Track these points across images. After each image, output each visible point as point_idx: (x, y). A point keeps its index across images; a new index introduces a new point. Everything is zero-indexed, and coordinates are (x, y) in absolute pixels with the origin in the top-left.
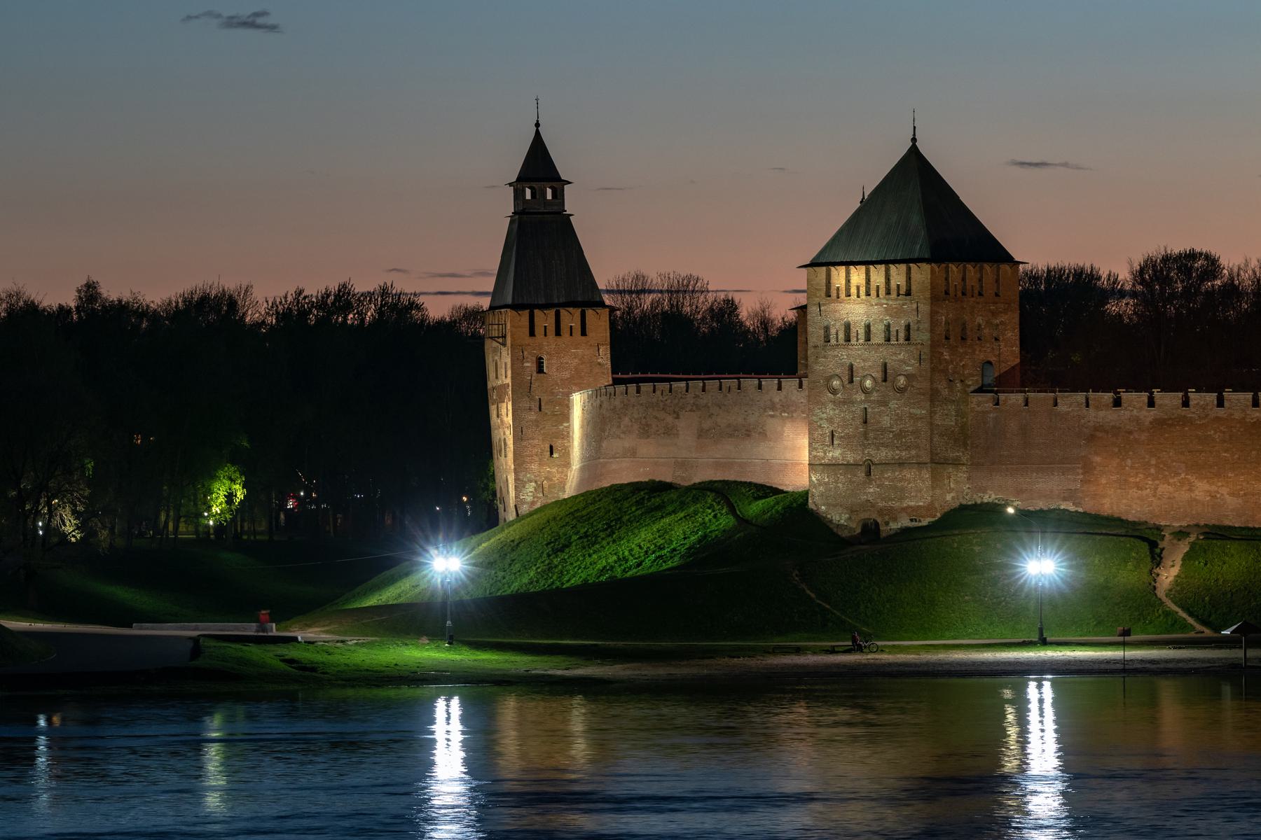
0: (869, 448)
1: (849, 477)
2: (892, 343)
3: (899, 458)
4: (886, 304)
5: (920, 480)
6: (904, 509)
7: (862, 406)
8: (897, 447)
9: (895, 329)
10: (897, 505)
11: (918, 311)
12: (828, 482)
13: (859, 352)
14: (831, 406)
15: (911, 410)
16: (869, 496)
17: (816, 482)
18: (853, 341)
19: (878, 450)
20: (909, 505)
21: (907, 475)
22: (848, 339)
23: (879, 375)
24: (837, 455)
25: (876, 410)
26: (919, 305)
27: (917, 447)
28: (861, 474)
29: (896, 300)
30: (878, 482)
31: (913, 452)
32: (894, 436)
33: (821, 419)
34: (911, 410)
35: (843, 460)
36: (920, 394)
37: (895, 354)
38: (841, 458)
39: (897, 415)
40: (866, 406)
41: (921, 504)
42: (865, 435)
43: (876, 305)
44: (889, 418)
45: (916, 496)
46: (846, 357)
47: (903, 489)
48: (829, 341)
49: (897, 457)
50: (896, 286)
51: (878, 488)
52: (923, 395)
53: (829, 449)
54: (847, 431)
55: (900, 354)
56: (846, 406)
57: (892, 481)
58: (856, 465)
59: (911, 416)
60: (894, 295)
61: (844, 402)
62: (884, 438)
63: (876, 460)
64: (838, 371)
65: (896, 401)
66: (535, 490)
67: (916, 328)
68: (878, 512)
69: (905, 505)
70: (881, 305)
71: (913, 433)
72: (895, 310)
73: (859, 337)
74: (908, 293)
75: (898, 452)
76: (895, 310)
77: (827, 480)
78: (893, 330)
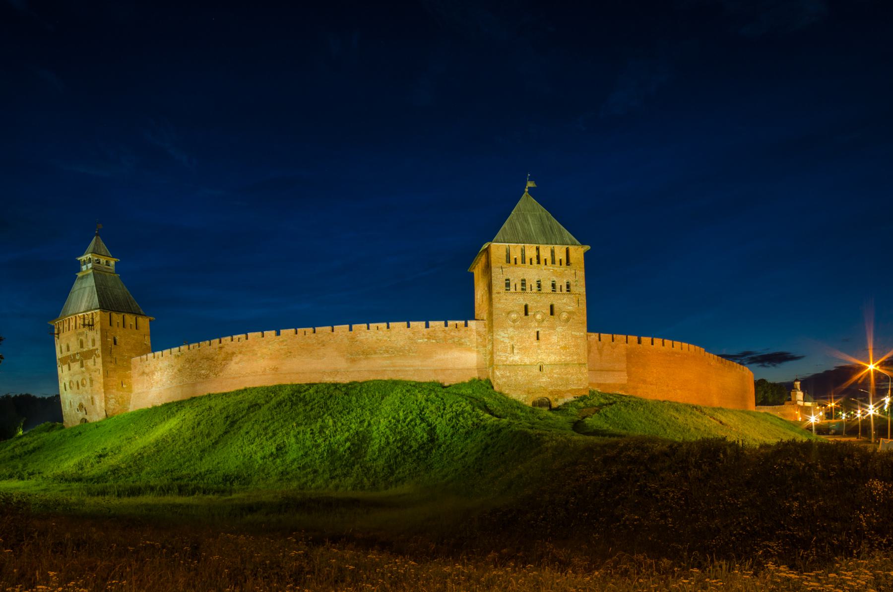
2: (557, 292)
3: (565, 361)
4: (553, 269)
6: (568, 391)
7: (537, 330)
9: (559, 285)
11: (575, 275)
12: (510, 377)
13: (533, 297)
14: (511, 329)
15: (573, 333)
16: (542, 383)
18: (528, 290)
25: (547, 332)
27: (578, 354)
29: (560, 267)
31: (575, 357)
33: (503, 337)
34: (573, 333)
35: (521, 362)
36: (580, 323)
37: (560, 299)
38: (520, 361)
39: (563, 335)
40: (538, 330)
41: (582, 388)
43: (545, 269)
45: (578, 383)
47: (567, 379)
49: (563, 360)
51: (549, 378)
52: (581, 324)
53: (510, 356)
54: (524, 345)
55: (563, 299)
57: (560, 374)
58: (531, 365)
61: (522, 327)
64: (516, 308)
65: (561, 327)
67: (574, 285)
68: (549, 393)
69: (569, 388)
70: (549, 270)
71: (574, 346)
73: (532, 288)
74: (568, 263)
75: (563, 357)
76: (559, 273)
77: (508, 374)
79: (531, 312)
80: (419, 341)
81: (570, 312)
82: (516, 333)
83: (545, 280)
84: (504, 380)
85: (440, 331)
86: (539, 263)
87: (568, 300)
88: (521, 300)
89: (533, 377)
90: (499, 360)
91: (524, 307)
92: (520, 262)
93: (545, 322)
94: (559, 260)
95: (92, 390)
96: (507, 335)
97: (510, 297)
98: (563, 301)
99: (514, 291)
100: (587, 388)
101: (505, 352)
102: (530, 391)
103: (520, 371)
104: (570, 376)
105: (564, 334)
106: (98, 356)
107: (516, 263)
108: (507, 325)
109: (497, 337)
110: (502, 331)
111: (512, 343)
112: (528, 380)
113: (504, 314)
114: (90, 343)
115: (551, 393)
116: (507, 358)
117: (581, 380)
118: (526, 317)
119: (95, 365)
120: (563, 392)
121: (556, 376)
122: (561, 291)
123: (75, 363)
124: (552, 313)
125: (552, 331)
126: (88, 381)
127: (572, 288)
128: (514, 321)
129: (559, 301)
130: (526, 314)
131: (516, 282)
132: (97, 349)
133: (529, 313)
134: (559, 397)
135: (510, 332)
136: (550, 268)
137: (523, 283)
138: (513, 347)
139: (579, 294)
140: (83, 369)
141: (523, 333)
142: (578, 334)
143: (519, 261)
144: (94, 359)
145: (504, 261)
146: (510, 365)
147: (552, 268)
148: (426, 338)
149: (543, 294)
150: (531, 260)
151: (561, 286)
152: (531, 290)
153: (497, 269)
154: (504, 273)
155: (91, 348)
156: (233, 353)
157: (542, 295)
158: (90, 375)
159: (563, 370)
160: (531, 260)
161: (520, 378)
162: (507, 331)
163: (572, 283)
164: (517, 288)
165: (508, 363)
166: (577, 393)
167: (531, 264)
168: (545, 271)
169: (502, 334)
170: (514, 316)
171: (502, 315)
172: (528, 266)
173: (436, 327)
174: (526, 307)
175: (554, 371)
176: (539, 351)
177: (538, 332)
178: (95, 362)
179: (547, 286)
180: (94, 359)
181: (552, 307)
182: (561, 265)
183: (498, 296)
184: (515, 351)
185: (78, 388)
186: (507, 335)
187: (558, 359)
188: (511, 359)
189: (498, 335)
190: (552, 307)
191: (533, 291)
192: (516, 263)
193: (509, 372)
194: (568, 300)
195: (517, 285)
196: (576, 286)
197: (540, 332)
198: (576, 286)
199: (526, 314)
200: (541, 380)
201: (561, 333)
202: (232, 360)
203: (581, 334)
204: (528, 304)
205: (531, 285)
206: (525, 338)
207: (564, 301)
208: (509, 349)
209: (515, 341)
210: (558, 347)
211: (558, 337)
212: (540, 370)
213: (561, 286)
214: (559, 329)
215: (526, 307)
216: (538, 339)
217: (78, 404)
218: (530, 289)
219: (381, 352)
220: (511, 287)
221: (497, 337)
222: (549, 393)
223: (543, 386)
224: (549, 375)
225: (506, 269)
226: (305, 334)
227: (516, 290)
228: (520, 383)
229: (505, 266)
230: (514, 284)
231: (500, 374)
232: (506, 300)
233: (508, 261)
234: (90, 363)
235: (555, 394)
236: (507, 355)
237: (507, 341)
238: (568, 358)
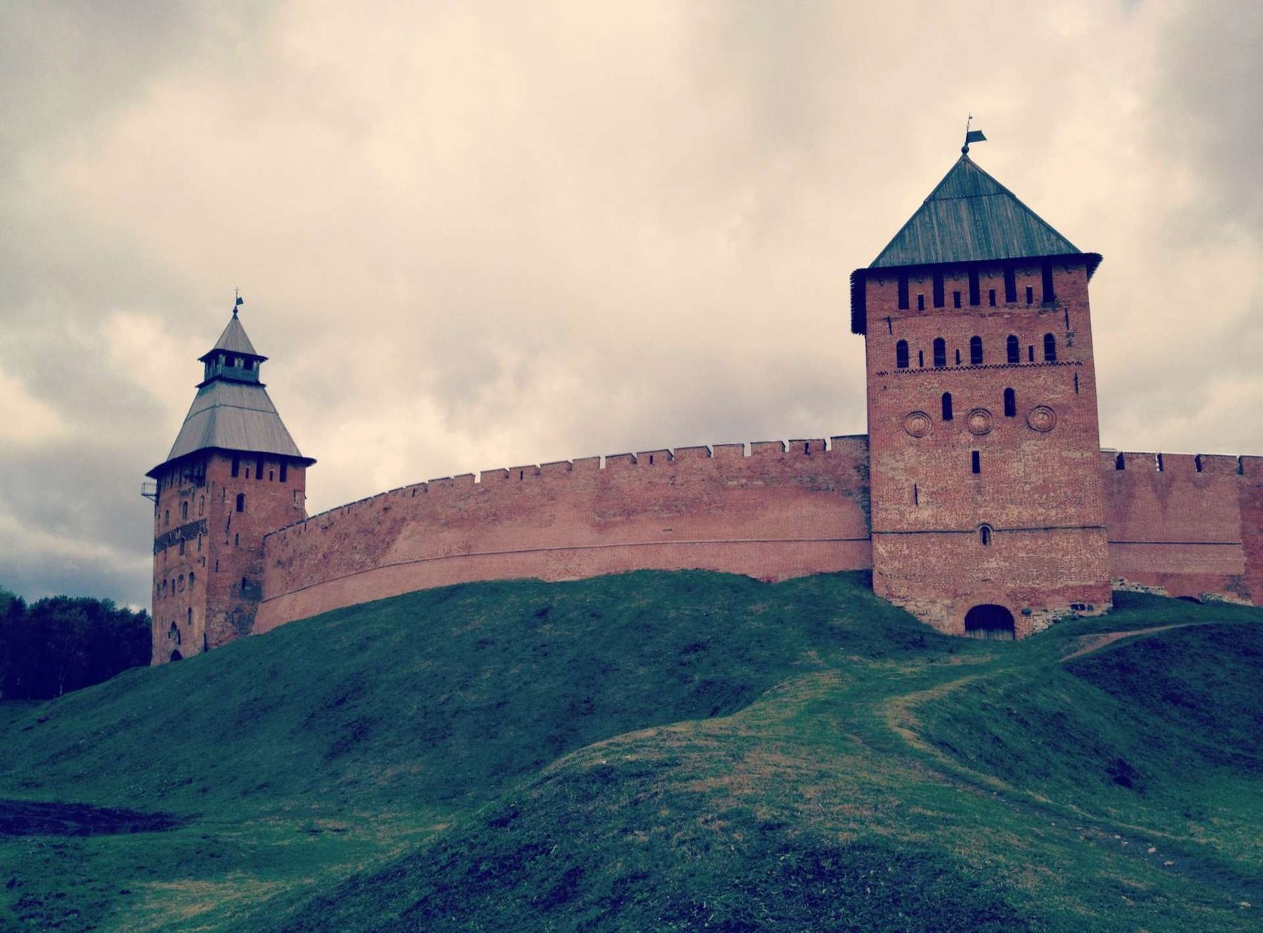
0: (986, 506)
1: (949, 546)
2: (1021, 364)
4: (1009, 314)
5: (1087, 549)
7: (971, 450)
8: (1039, 504)
10: (1045, 586)
13: (962, 379)
17: (885, 555)
18: (951, 362)
19: (1004, 508)
20: (1066, 585)
21: (1060, 543)
22: (940, 361)
23: (1000, 408)
24: (926, 517)
26: (1069, 312)
27: (1080, 503)
28: (974, 542)
29: (1027, 307)
30: (1005, 553)
31: (1072, 511)
32: (1032, 489)
34: (1064, 454)
37: (1028, 378)
38: (933, 521)
39: (1039, 459)
40: (976, 449)
41: (1092, 583)
42: (979, 489)
43: (990, 315)
44: (1023, 464)
45: (1080, 572)
46: (937, 386)
47: (1052, 561)
48: (907, 365)
50: (1025, 290)
53: (908, 510)
56: (940, 451)
57: (1034, 552)
59: (1063, 461)
60: (1022, 301)
62: (1014, 492)
63: (997, 524)
64: (922, 406)
65: (1034, 442)
66: (226, 620)
67: (1065, 342)
68: (1008, 596)
72: (1025, 321)
73: (961, 358)
74: (1049, 297)
75: (1041, 510)
76: (1025, 321)
77: (906, 552)
78: (1023, 347)
79: (956, 411)
80: (730, 483)
81: (1054, 405)
82: (923, 458)
83: (991, 339)
84: (896, 564)
85: (772, 460)
86: (975, 300)
87: (1050, 380)
88: (935, 385)
89: (966, 558)
90: (883, 521)
91: (940, 401)
92: (932, 305)
93: (994, 433)
94: (1025, 291)
95: (190, 596)
96: (901, 465)
97: (908, 381)
98: (1036, 382)
99: (918, 367)
100: (1107, 584)
101: (899, 501)
102: (960, 591)
103: (933, 544)
104: (1059, 556)
105: (1042, 456)
106: (205, 532)
107: (921, 307)
108: (902, 441)
109: (882, 469)
110: (891, 456)
111: (913, 481)
112: (955, 566)
113: (894, 419)
114: (197, 510)
115: (1012, 595)
116: (902, 514)
117: (1089, 566)
118: (946, 423)
119: (199, 549)
120: (1044, 592)
121: (1024, 554)
122: (1031, 359)
123: (173, 547)
124: (1010, 410)
125: (1011, 451)
126: (187, 578)
127: (1062, 353)
128: (918, 434)
129: (1027, 383)
130: (947, 415)
131: (921, 347)
132: (206, 520)
133: (954, 414)
134: (1032, 605)
135: (909, 459)
136: (1003, 311)
137: (939, 345)
138: (916, 489)
139: (1079, 363)
140: (183, 558)
141: (939, 457)
142: (1077, 455)
143: (929, 304)
144: (200, 538)
145: (894, 304)
146: (911, 533)
147: (1007, 310)
148: (743, 477)
149: (987, 370)
150: (957, 296)
151: (1031, 348)
152: (958, 362)
153: (880, 324)
154: (895, 331)
155: (197, 518)
156: (403, 519)
157: (984, 372)
158: (191, 568)
159: (1040, 542)
160: (957, 296)
161: (933, 560)
162: (902, 454)
163: (1060, 340)
164: (925, 361)
165: (904, 526)
166: (1080, 597)
167: (958, 305)
168: (990, 318)
169: (891, 462)
170: (918, 423)
171: (889, 419)
172: (951, 312)
173: (765, 454)
174: (947, 399)
175: (1019, 544)
176: (979, 498)
177: (976, 456)
178: (200, 544)
179: (995, 351)
180: (200, 538)
181: (1009, 394)
182: (1030, 300)
183: (881, 379)
184: (921, 499)
185: (173, 595)
186: (901, 465)
187: (1026, 515)
188: (913, 516)
189: (883, 464)
190: (1009, 394)
191: (961, 364)
192: (921, 307)
193: (908, 548)
194: (1050, 380)
195: (924, 355)
196: (1070, 344)
197: (980, 455)
198: (1070, 344)
199: (947, 415)
200: (986, 565)
201: (1032, 454)
202: (400, 532)
203: (1085, 455)
204: (951, 392)
205: (958, 351)
206: (945, 469)
207: (1041, 381)
208: (906, 495)
209: (921, 476)
210: (1027, 488)
211: (1026, 465)
212: (985, 542)
213: (1031, 348)
214: (1029, 446)
215: (947, 399)
216: (976, 468)
217: (171, 622)
218: (955, 362)
219: (656, 508)
220: (910, 360)
221: (882, 469)
222: (1008, 596)
223: (991, 578)
224: (1005, 553)
225: (900, 322)
226: (521, 478)
227: (921, 365)
228: (933, 570)
229: (897, 315)
230: (917, 352)
231: (887, 552)
232: (899, 387)
233: (903, 304)
234: (192, 545)
235: (1023, 599)
236: (903, 508)
237: (901, 476)
238: (1053, 513)
